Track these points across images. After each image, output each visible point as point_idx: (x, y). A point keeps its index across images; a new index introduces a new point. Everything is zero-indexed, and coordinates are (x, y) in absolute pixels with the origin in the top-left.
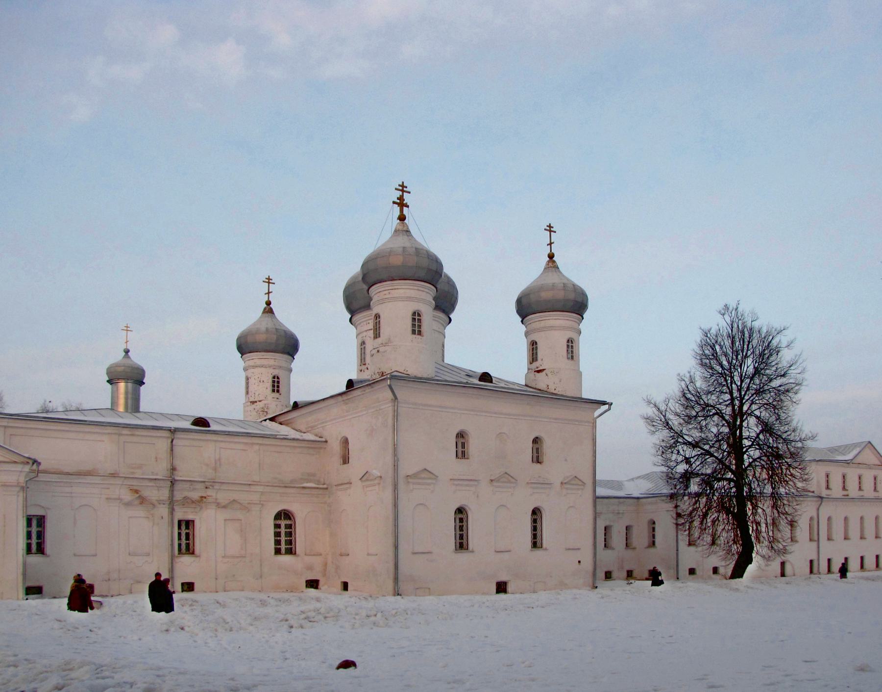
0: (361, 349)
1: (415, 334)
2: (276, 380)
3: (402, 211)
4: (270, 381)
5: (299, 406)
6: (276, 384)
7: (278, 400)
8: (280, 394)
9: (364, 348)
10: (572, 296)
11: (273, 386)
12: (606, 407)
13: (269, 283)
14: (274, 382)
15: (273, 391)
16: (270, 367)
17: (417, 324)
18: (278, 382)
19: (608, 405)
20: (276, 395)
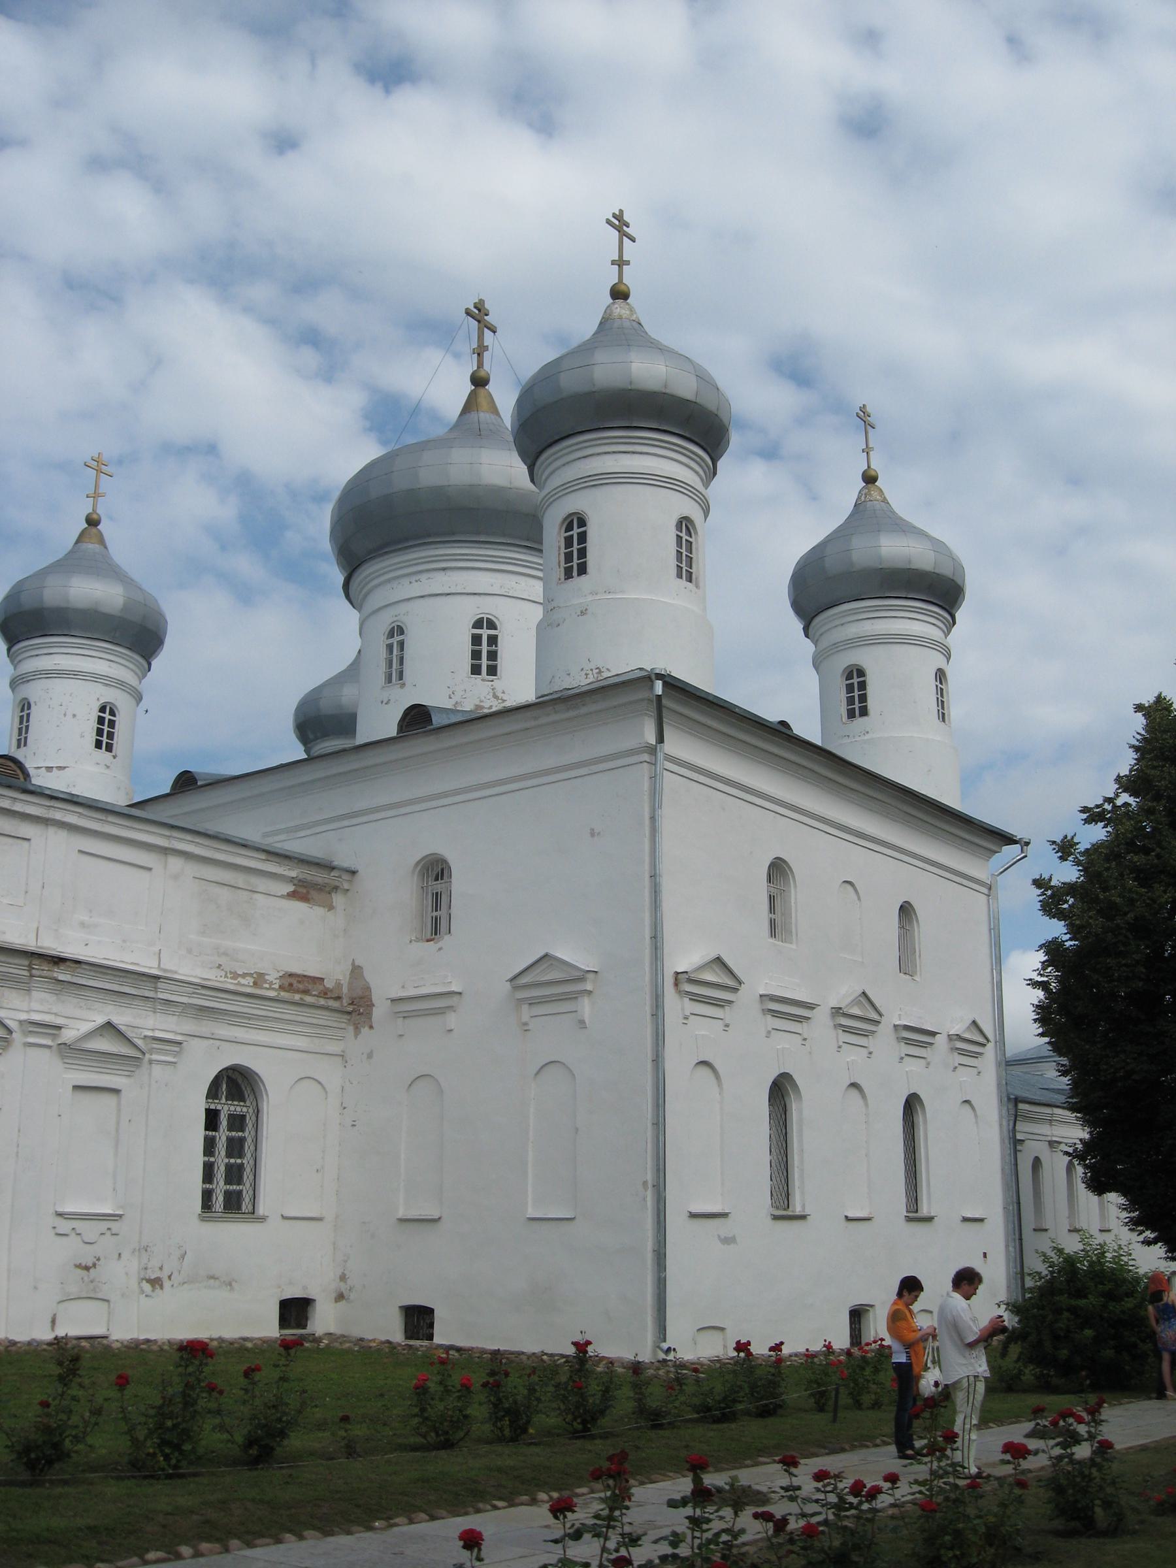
0: (390, 647)
1: (681, 578)
2: (107, 716)
3: (481, 336)
4: (95, 714)
5: (199, 783)
6: (106, 728)
7: (107, 771)
8: (114, 757)
9: (401, 644)
10: (946, 570)
11: (100, 732)
12: (1012, 851)
13: (99, 471)
14: (101, 721)
15: (98, 745)
16: (95, 678)
17: (684, 553)
18: (112, 724)
19: (1018, 846)
20: (102, 754)
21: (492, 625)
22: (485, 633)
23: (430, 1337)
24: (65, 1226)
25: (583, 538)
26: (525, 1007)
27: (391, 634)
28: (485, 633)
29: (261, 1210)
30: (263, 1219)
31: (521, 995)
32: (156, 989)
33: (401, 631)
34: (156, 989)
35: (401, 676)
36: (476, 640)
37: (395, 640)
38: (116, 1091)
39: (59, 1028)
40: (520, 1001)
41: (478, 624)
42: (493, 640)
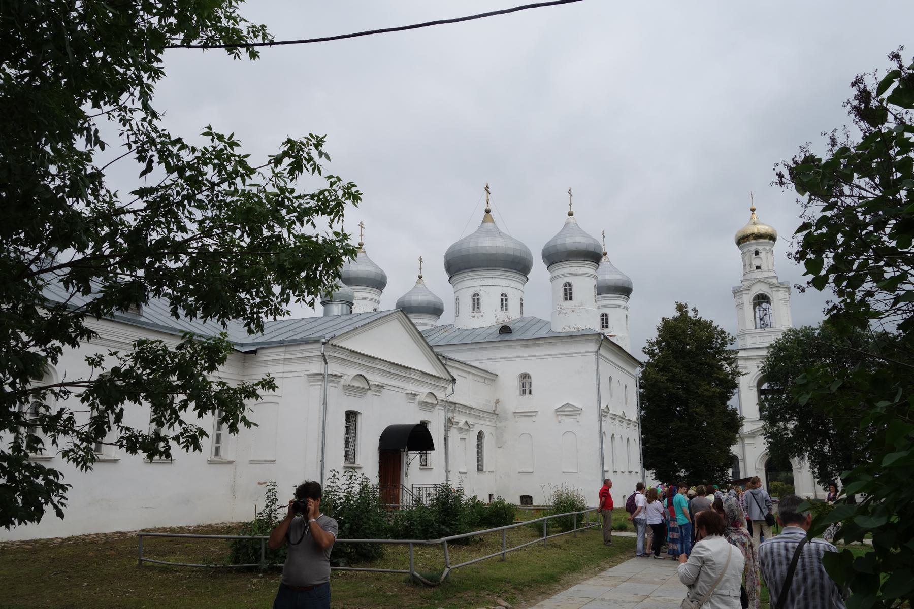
0: (474, 300)
13: (362, 227)
21: (506, 296)
22: (504, 298)
23: (532, 504)
24: (460, 475)
25: (570, 289)
26: (559, 417)
27: (474, 295)
28: (504, 298)
29: (485, 469)
30: (485, 472)
31: (558, 413)
32: (471, 411)
33: (478, 295)
34: (471, 411)
35: (478, 308)
36: (502, 300)
37: (476, 298)
38: (464, 439)
39: (458, 423)
40: (558, 415)
41: (502, 295)
42: (506, 300)
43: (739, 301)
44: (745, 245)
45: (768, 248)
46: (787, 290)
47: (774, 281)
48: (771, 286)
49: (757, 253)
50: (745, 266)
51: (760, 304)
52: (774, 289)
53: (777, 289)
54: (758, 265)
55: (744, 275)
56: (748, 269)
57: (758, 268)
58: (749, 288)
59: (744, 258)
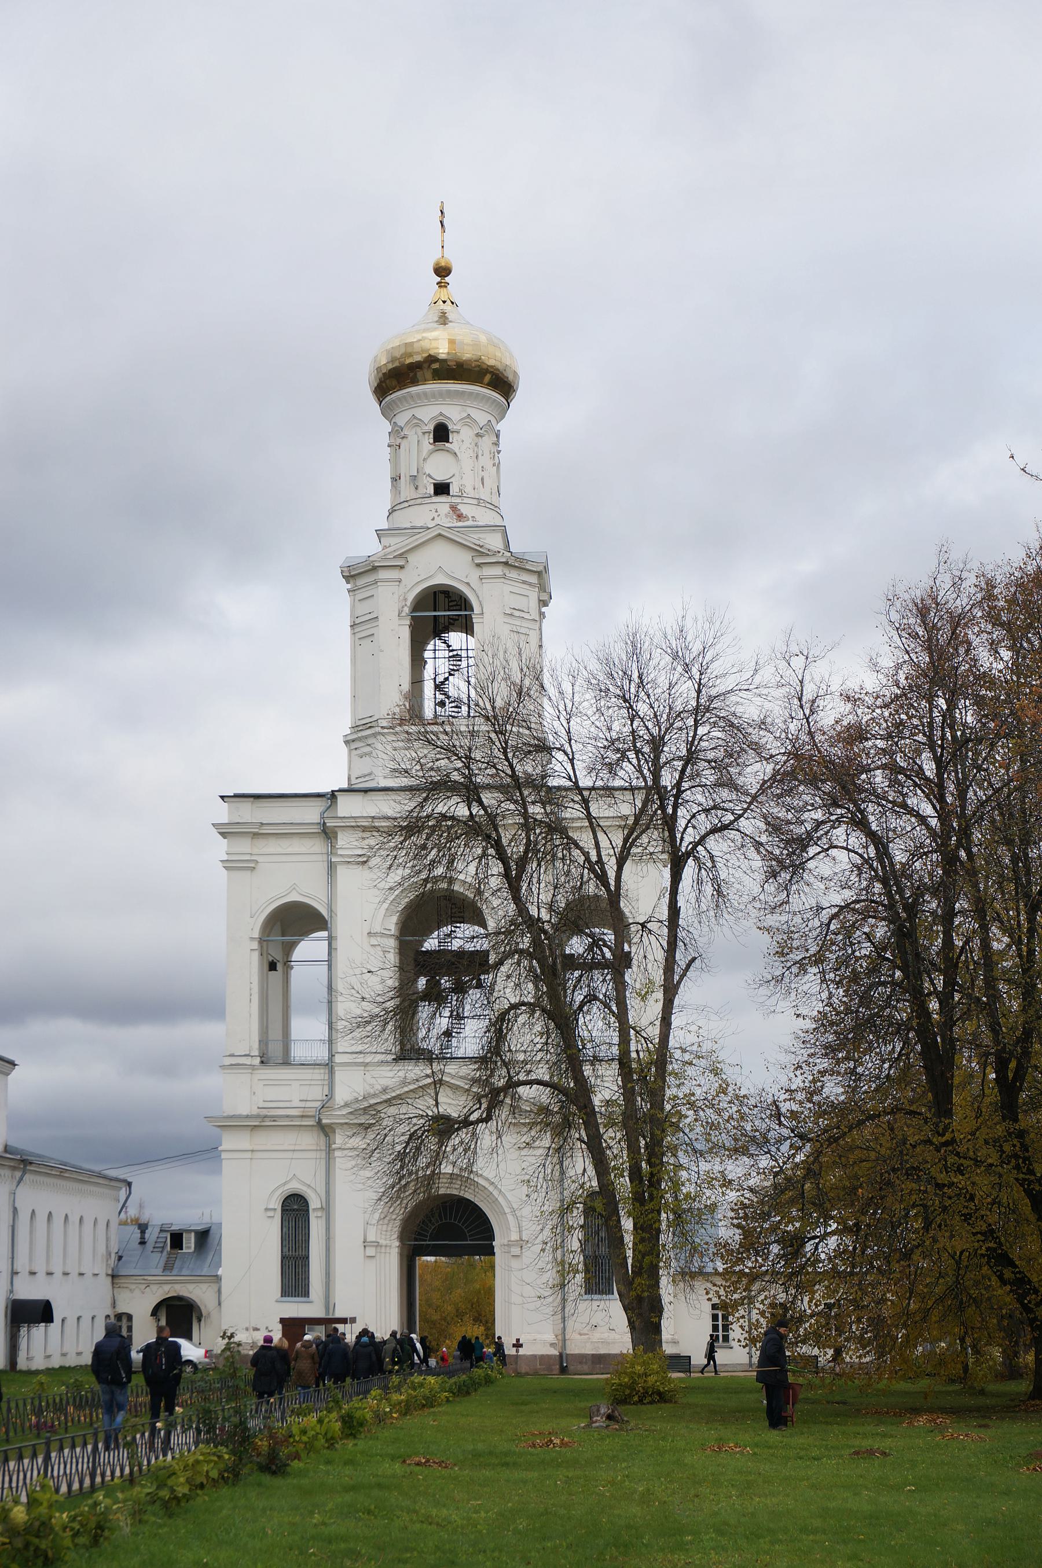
43: (363, 608)
44: (404, 398)
45: (482, 417)
46: (533, 579)
47: (494, 542)
48: (480, 555)
49: (441, 433)
50: (395, 479)
51: (440, 629)
52: (488, 571)
53: (498, 571)
54: (441, 478)
55: (392, 511)
56: (407, 491)
57: (442, 489)
58: (400, 562)
59: (395, 447)
